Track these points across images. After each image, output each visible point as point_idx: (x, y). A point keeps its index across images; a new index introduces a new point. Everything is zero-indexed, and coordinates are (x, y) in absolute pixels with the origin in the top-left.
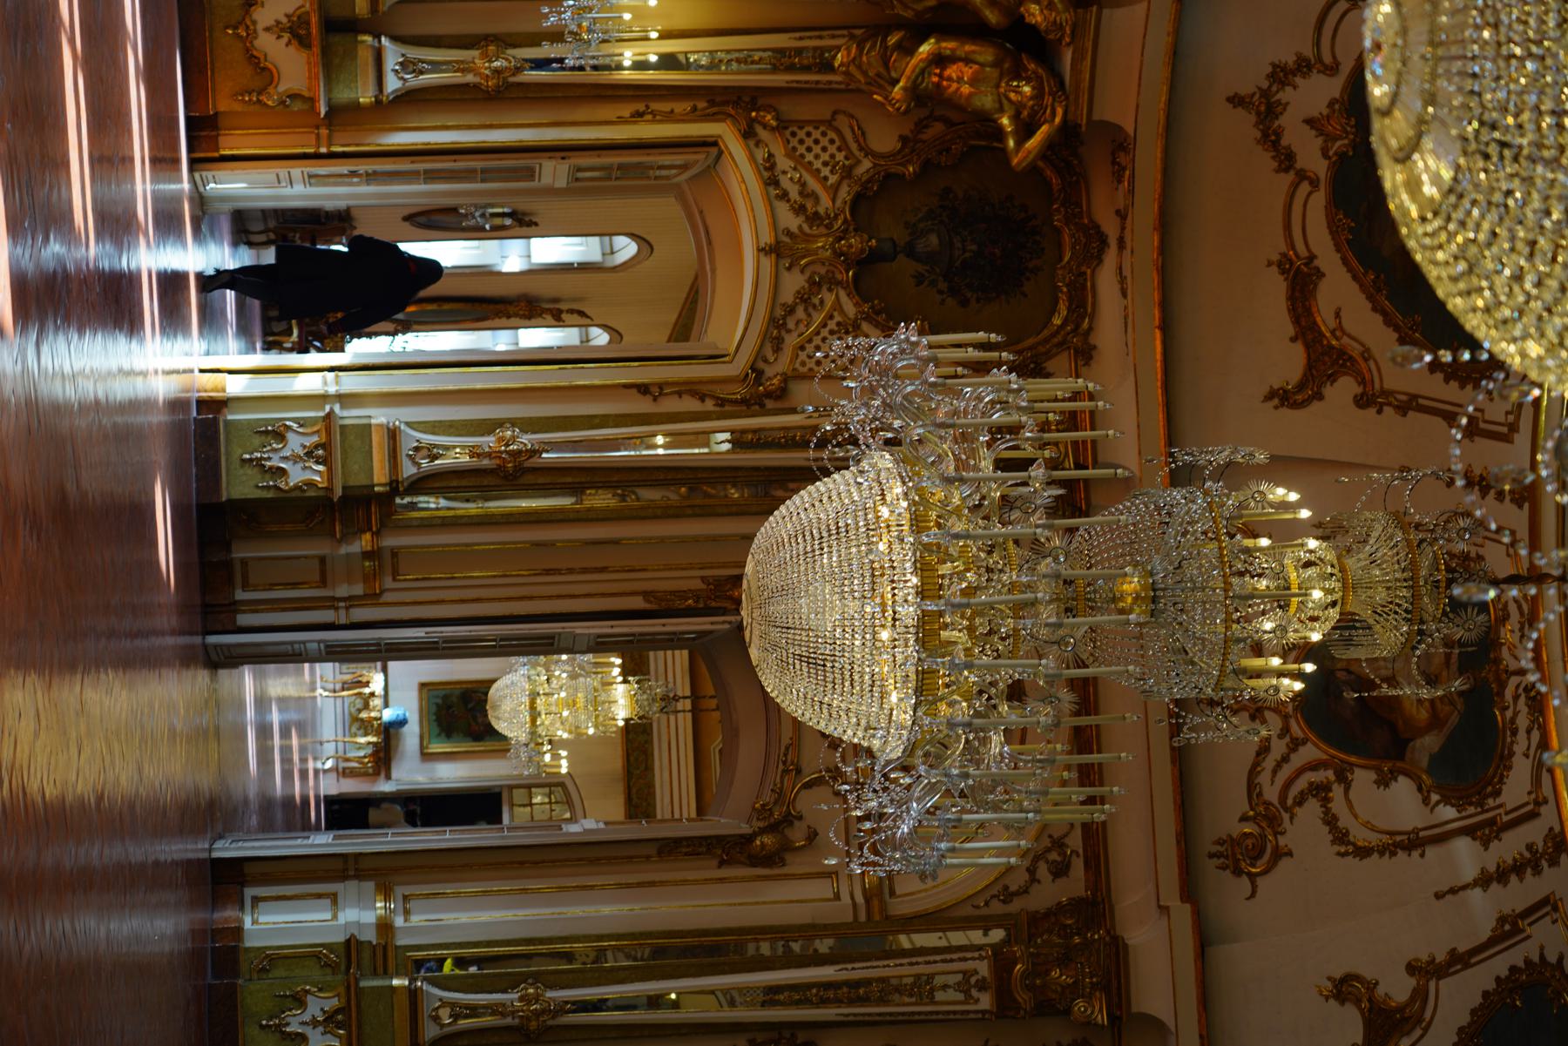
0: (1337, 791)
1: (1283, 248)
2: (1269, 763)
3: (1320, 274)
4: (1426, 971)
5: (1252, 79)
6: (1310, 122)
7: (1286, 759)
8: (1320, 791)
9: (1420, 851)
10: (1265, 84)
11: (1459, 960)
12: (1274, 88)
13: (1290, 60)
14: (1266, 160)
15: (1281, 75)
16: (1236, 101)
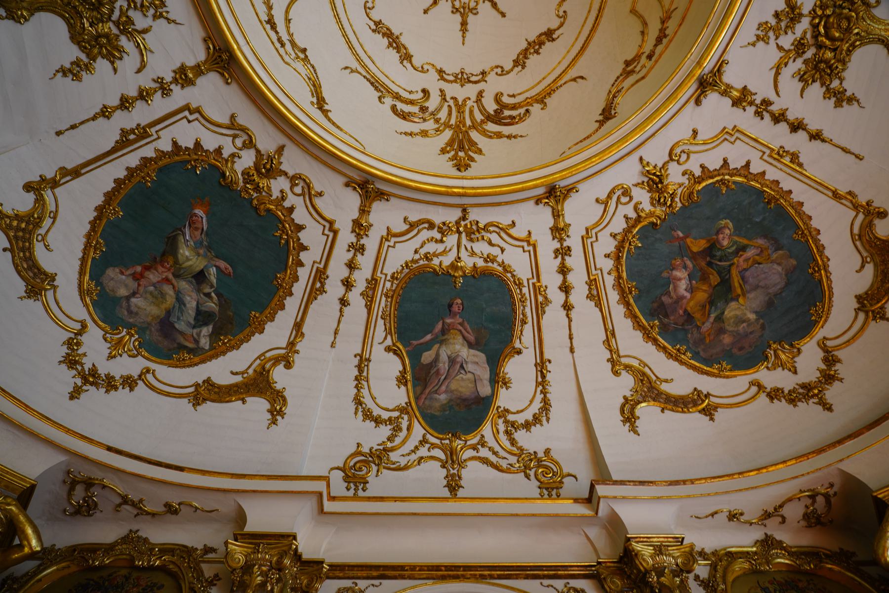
0: (511, 417)
1: (186, 400)
2: (493, 459)
3: (208, 381)
4: (616, 364)
5: (68, 378)
6: (111, 357)
7: (490, 449)
8: (512, 427)
9: (547, 363)
10: (74, 372)
11: (610, 334)
12: (79, 368)
13: (64, 350)
14: (123, 393)
15: (71, 361)
16: (75, 394)
